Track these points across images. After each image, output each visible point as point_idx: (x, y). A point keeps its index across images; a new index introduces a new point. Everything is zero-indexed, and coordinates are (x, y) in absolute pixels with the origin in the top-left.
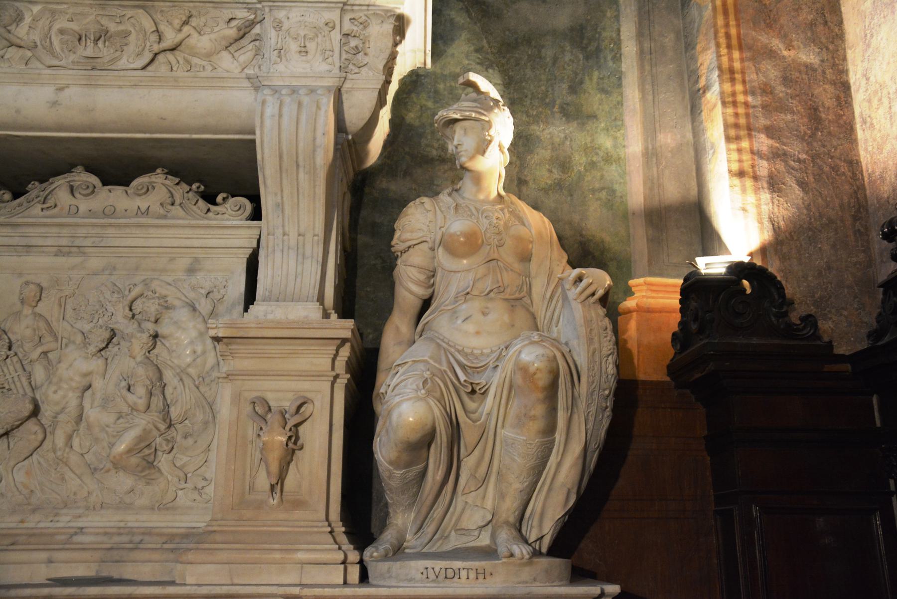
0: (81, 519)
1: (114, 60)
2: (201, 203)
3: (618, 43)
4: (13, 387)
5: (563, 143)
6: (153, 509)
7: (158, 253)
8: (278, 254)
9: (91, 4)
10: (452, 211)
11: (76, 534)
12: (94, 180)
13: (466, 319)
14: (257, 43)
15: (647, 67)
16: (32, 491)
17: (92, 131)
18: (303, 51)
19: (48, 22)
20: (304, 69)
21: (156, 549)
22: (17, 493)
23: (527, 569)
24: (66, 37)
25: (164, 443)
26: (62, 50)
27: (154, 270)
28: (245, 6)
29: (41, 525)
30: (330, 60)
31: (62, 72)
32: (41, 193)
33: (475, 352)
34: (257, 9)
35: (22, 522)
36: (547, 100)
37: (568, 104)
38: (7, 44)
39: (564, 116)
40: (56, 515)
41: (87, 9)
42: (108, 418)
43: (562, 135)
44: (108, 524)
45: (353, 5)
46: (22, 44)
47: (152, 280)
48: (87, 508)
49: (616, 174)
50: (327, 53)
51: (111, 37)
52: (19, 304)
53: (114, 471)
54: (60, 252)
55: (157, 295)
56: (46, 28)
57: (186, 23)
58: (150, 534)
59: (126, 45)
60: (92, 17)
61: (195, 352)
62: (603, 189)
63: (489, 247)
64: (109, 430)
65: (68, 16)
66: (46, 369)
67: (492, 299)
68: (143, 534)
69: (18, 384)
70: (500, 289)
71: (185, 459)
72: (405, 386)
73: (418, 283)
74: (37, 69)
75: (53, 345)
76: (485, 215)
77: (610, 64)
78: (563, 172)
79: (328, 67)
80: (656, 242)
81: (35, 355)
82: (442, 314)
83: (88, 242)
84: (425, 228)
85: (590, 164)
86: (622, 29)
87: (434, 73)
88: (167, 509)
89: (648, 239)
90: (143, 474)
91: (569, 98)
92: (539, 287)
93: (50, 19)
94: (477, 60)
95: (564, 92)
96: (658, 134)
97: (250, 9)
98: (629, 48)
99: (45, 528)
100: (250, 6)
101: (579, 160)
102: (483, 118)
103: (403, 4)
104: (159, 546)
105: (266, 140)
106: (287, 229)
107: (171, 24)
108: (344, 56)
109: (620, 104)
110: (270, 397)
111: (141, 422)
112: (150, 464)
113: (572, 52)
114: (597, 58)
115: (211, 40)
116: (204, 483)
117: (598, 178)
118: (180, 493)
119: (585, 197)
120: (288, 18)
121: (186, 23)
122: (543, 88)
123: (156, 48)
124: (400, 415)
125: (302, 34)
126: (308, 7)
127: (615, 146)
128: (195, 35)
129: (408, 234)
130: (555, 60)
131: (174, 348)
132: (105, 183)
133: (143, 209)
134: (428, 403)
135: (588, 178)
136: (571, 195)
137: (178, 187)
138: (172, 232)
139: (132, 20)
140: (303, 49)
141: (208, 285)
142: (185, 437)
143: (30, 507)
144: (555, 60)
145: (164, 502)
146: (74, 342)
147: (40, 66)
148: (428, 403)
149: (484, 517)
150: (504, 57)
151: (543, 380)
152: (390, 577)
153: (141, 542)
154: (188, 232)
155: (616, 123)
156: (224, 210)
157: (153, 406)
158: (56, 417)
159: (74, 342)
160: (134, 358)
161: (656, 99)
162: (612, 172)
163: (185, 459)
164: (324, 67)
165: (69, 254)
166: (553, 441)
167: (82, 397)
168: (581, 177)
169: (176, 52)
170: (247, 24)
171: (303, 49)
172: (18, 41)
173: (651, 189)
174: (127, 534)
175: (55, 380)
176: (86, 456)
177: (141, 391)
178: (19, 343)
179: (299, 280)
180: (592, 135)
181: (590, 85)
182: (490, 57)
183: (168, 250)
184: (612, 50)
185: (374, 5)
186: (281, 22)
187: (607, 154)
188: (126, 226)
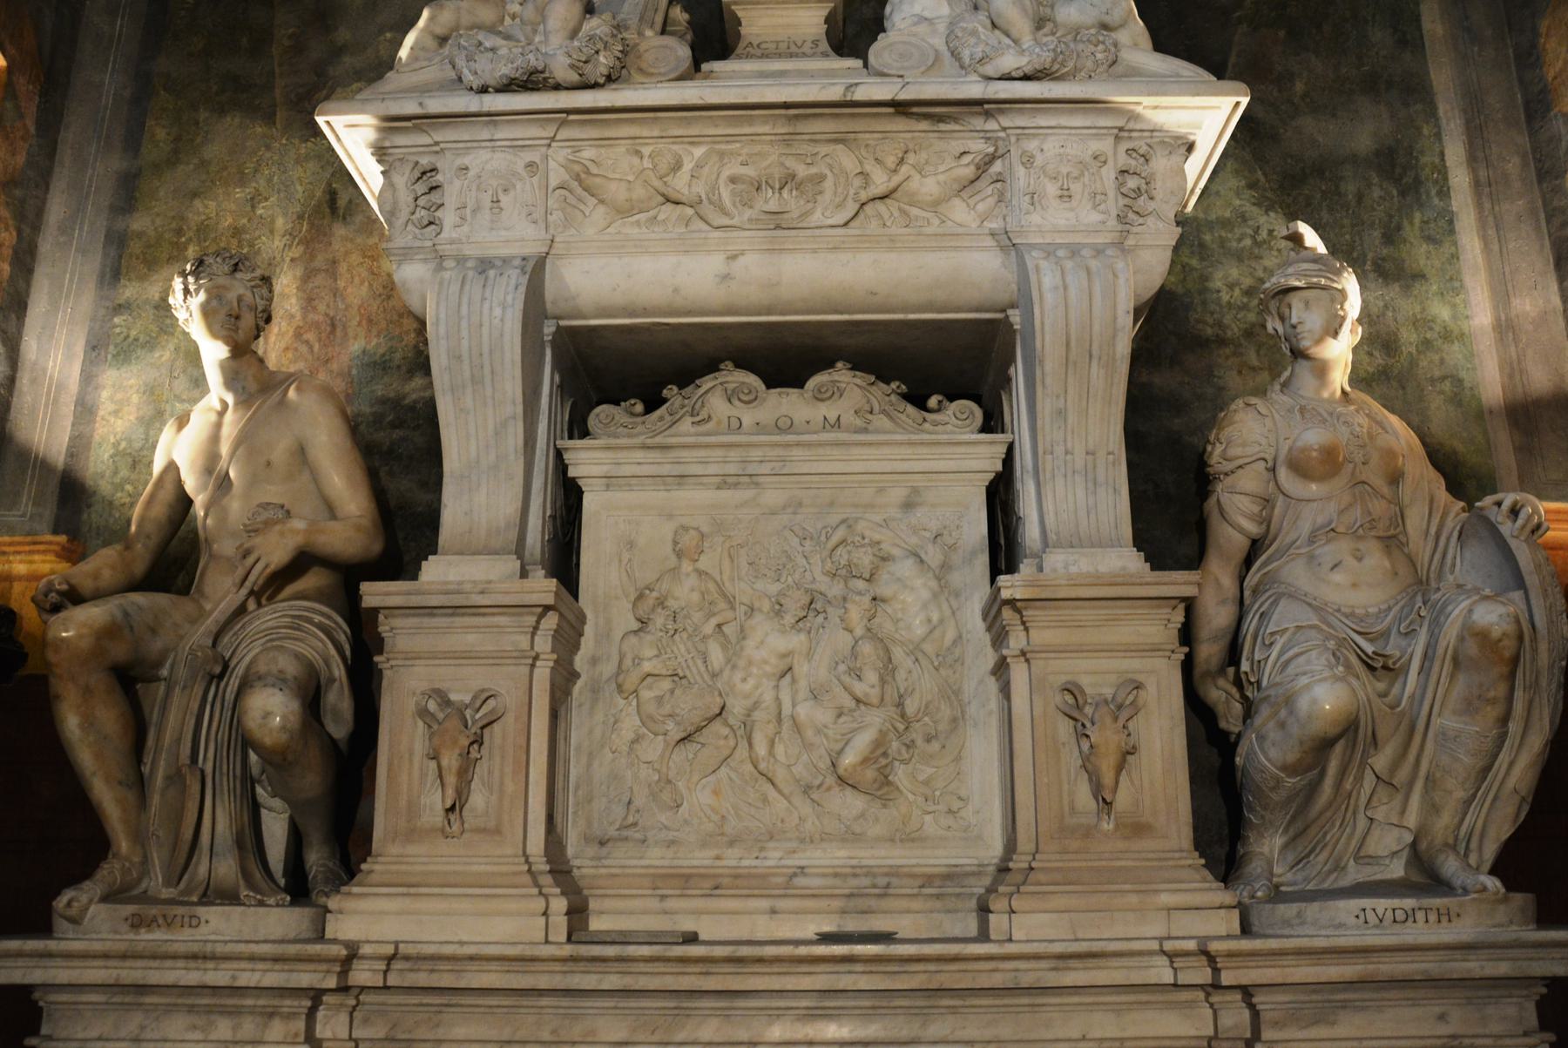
0: (796, 856)
1: (805, 215)
2: (911, 409)
3: (1443, 171)
4: (688, 673)
5: (1384, 315)
6: (892, 840)
7: (860, 482)
8: (1060, 481)
10: (1298, 416)
11: (795, 875)
12: (753, 380)
13: (1336, 566)
14: (999, 185)
15: (1487, 205)
16: (723, 817)
17: (769, 313)
18: (1065, 196)
21: (914, 895)
22: (705, 820)
23: (1502, 908)
24: (740, 187)
25: (904, 750)
26: (734, 205)
27: (856, 506)
28: (982, 135)
29: (746, 863)
30: (1102, 207)
31: (735, 234)
32: (686, 401)
33: (1357, 611)
34: (997, 139)
35: (718, 858)
36: (1355, 255)
37: (1383, 259)
38: (661, 199)
39: (1379, 276)
40: (762, 849)
41: (766, 148)
42: (824, 716)
43: (1381, 304)
44: (836, 862)
46: (684, 199)
47: (857, 520)
48: (802, 841)
49: (1460, 356)
50: (1098, 197)
51: (801, 184)
52: (673, 558)
53: (837, 789)
54: (724, 483)
55: (866, 541)
58: (897, 875)
59: (821, 193)
60: (773, 158)
61: (929, 621)
62: (1444, 378)
63: (1351, 465)
64: (830, 733)
65: (740, 159)
66: (724, 648)
67: (1361, 538)
68: (887, 875)
69: (694, 669)
70: (1373, 523)
71: (930, 771)
72: (1309, 662)
73: (1251, 518)
74: (700, 231)
75: (729, 615)
76: (1342, 419)
77: (1436, 201)
78: (1389, 355)
79: (1101, 217)
80: (1526, 451)
81: (709, 628)
82: (1293, 560)
83: (766, 469)
84: (1264, 442)
85: (1423, 343)
86: (1446, 152)
87: (1195, 218)
88: (913, 840)
89: (1514, 448)
90: (879, 793)
91: (1385, 251)
92: (1415, 520)
94: (1253, 200)
95: (1377, 242)
96: (1512, 299)
97: (989, 139)
98: (1460, 178)
99: (750, 867)
100: (988, 135)
101: (1409, 338)
102: (1335, 285)
103: (1199, 127)
104: (915, 891)
105: (1047, 322)
106: (1069, 445)
108: (1122, 201)
109: (1455, 257)
110: (1085, 681)
111: (875, 721)
112: (885, 781)
113: (1381, 186)
114: (1417, 192)
115: (938, 183)
116: (961, 804)
117: (1437, 362)
118: (928, 818)
119: (1422, 390)
122: (1347, 237)
123: (864, 196)
124: (1314, 701)
125: (1064, 170)
127: (1454, 317)
128: (917, 177)
129: (1240, 449)
130: (1360, 197)
131: (900, 615)
132: (769, 386)
133: (832, 418)
134: (1349, 684)
135: (1424, 363)
136: (1404, 388)
137: (874, 387)
138: (886, 450)
139: (828, 160)
140: (1066, 193)
141: (934, 526)
142: (928, 740)
143: (725, 839)
144: (1360, 197)
145: (908, 831)
146: (760, 610)
147: (706, 227)
148: (1349, 684)
149: (1399, 840)
150: (1289, 195)
151: (1508, 648)
152: (1303, 923)
153: (888, 886)
154: (907, 451)
155: (1453, 285)
156: (947, 419)
157: (887, 698)
158: (749, 715)
159: (760, 610)
160: (851, 632)
161: (1504, 250)
162: (1455, 353)
163: (930, 771)
164: (1095, 217)
165: (736, 485)
166: (1507, 732)
167: (777, 687)
168: (1413, 363)
169: (888, 201)
170: (987, 159)
171: (1066, 193)
173: (1511, 376)
174: (866, 875)
175: (742, 663)
176: (793, 768)
177: (872, 677)
178: (685, 612)
179: (1093, 516)
180: (1422, 303)
181: (1411, 231)
182: (1269, 194)
183: (877, 477)
184: (1436, 182)
185: (1160, 131)
186: (1032, 156)
187: (1445, 328)
188: (820, 444)
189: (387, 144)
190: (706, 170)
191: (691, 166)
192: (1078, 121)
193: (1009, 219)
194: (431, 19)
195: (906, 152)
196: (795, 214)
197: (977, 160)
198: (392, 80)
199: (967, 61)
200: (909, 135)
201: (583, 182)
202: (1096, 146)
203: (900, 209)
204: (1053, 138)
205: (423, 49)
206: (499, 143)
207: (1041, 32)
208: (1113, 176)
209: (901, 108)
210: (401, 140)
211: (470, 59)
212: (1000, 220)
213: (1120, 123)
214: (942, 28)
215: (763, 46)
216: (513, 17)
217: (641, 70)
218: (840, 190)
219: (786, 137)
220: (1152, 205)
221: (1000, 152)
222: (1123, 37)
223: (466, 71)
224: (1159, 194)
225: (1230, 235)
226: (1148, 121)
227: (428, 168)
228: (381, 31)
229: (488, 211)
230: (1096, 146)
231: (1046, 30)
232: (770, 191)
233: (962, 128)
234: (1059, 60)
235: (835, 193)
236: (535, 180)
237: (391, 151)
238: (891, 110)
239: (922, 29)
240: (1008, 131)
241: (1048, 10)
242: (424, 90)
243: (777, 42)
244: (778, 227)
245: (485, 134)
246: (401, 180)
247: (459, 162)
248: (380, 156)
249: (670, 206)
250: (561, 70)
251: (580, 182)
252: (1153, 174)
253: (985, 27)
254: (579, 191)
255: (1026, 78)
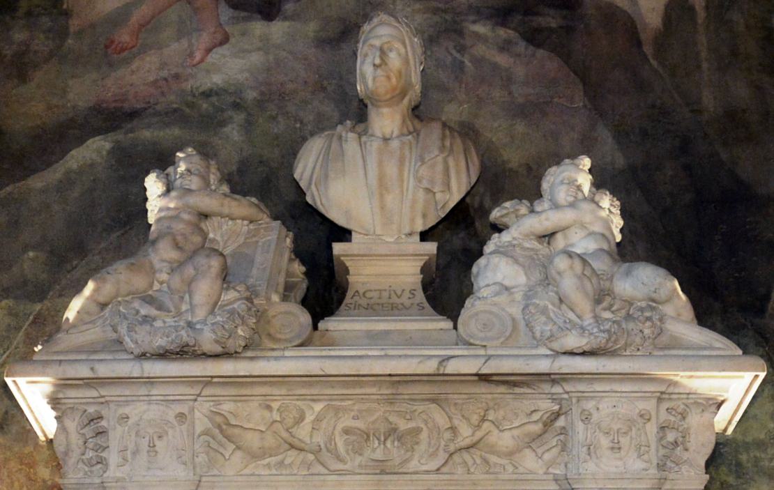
1: (407, 461)
9: (378, 399)
14: (562, 437)
18: (616, 448)
19: (332, 422)
20: (616, 467)
24: (353, 438)
26: (347, 451)
28: (549, 396)
30: (646, 457)
34: (562, 399)
38: (287, 446)
41: (375, 405)
45: (672, 394)
46: (306, 448)
50: (643, 448)
51: (401, 437)
56: (331, 429)
57: (483, 420)
59: (417, 443)
65: (352, 414)
79: (644, 465)
93: (334, 420)
100: (554, 397)
103: (727, 392)
107: (468, 419)
108: (662, 452)
115: (513, 437)
120: (598, 409)
121: (483, 420)
123: (452, 448)
125: (615, 427)
126: (621, 397)
128: (496, 432)
140: (616, 446)
147: (324, 471)
164: (639, 465)
169: (472, 450)
170: (553, 417)
171: (616, 446)
172: (297, 443)
185: (695, 394)
186: (590, 414)
189: (61, 395)
190: (324, 424)
191: (312, 418)
192: (627, 387)
193: (570, 466)
194: (96, 290)
195: (487, 410)
196: (397, 461)
197: (545, 418)
198: (65, 340)
199: (538, 334)
200: (489, 396)
201: (224, 430)
202: (641, 405)
203: (481, 456)
204: (606, 399)
205: (88, 313)
206: (154, 398)
207: (601, 306)
208: (655, 430)
209: (484, 378)
210: (72, 393)
211: (130, 329)
212: (563, 465)
213: (663, 389)
214: (519, 296)
215: (368, 295)
216: (161, 283)
217: (269, 335)
218: (433, 442)
219: (391, 397)
220: (686, 456)
221: (564, 410)
222: (668, 310)
223: (127, 339)
224: (692, 445)
225: (763, 456)
226: (684, 387)
227: (96, 417)
228: (26, 248)
229: (146, 454)
230: (641, 405)
231: (605, 304)
232: (376, 442)
233: (533, 391)
234: (613, 339)
235: (430, 444)
236: (184, 427)
237: (63, 401)
238: (476, 378)
239: (503, 299)
240: (571, 394)
241: (607, 284)
242: (92, 349)
243: (380, 290)
244: (383, 472)
245: (143, 391)
246: (72, 425)
247: (121, 411)
248: (54, 404)
249: (293, 453)
250: (207, 341)
251: (222, 431)
252: (688, 429)
253: (553, 304)
254: (220, 437)
255: (584, 354)
